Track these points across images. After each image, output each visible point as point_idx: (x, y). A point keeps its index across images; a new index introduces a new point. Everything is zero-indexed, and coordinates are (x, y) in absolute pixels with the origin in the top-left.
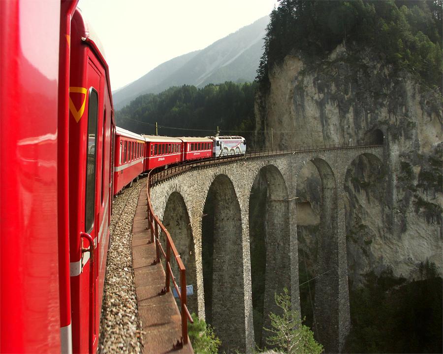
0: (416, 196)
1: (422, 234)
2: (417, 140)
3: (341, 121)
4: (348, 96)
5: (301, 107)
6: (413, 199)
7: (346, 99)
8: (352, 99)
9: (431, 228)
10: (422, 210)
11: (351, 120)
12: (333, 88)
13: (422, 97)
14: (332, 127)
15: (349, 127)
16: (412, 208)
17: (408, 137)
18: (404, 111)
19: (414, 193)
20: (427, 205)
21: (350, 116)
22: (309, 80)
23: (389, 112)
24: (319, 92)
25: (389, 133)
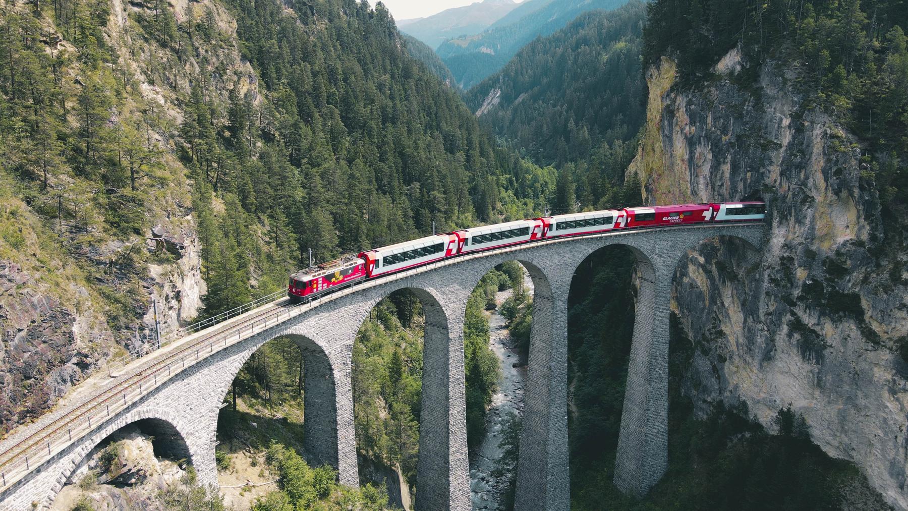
0: (793, 314)
1: (792, 370)
2: (812, 228)
3: (711, 173)
5: (669, 139)
6: (789, 316)
8: (731, 143)
9: (807, 367)
10: (797, 336)
11: (727, 175)
12: (709, 120)
13: (829, 160)
14: (702, 180)
15: (722, 185)
16: (785, 329)
17: (799, 221)
18: (802, 176)
21: (726, 168)
22: (681, 101)
23: (781, 174)
24: (691, 124)
25: (774, 209)
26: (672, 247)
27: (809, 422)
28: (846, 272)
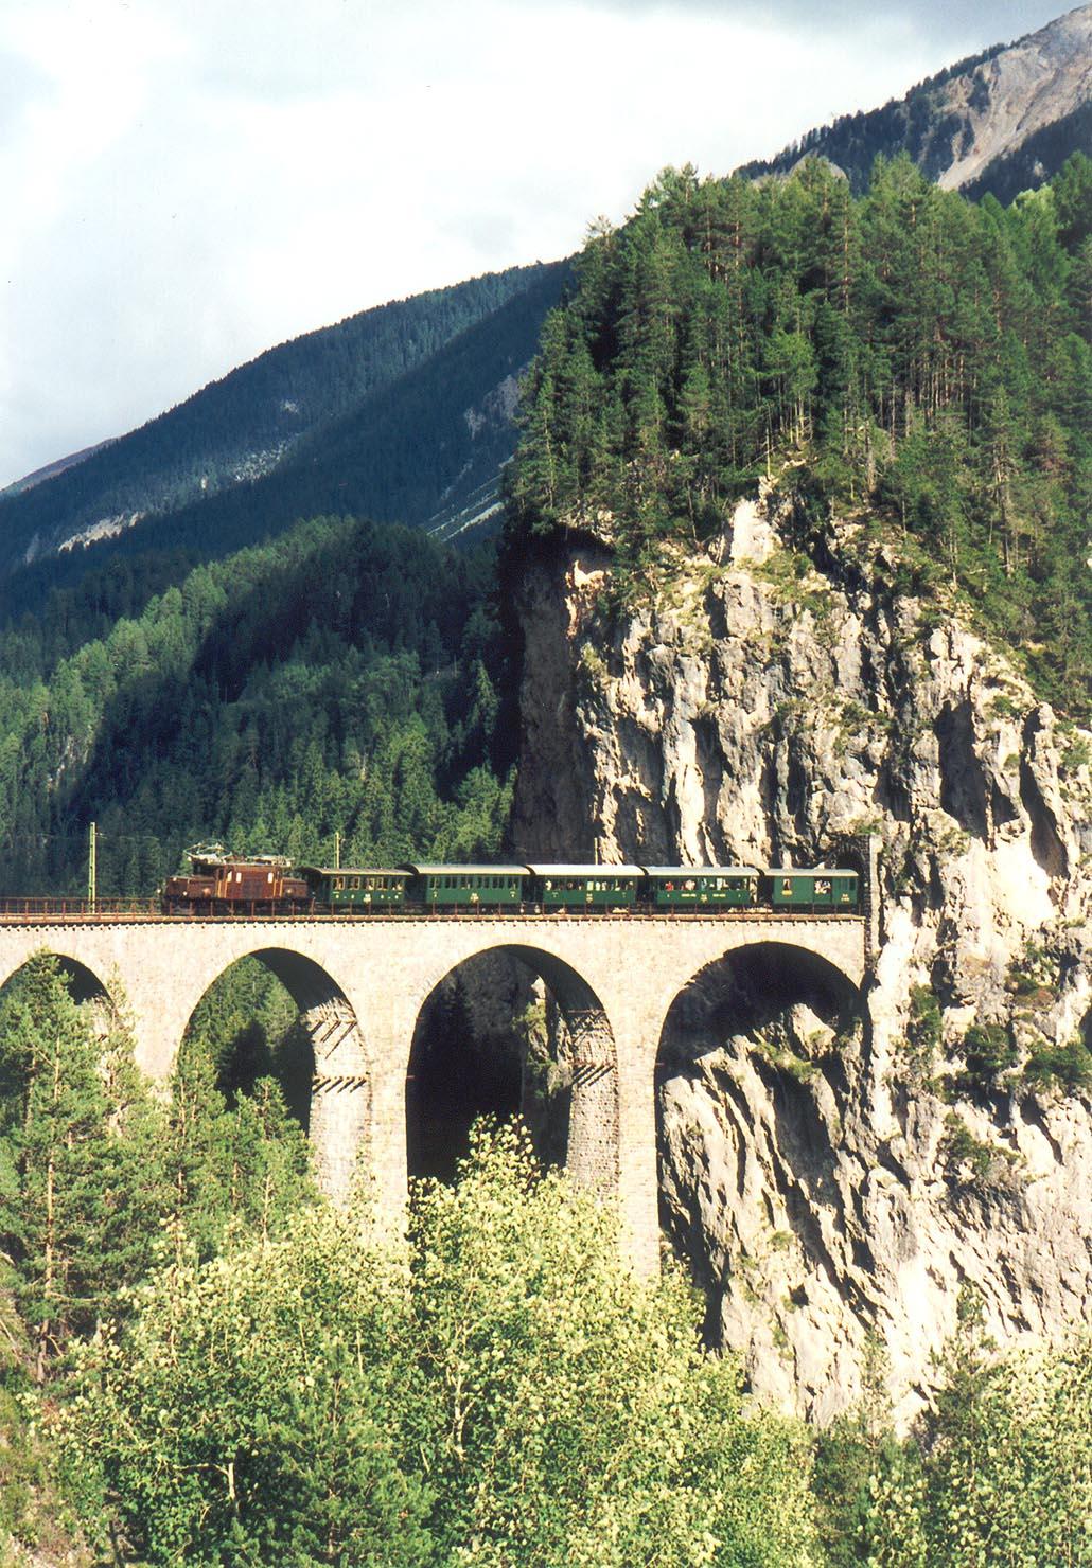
4: (753, 716)
7: (748, 728)
9: (995, 1242)
19: (948, 1109)
20: (983, 1154)
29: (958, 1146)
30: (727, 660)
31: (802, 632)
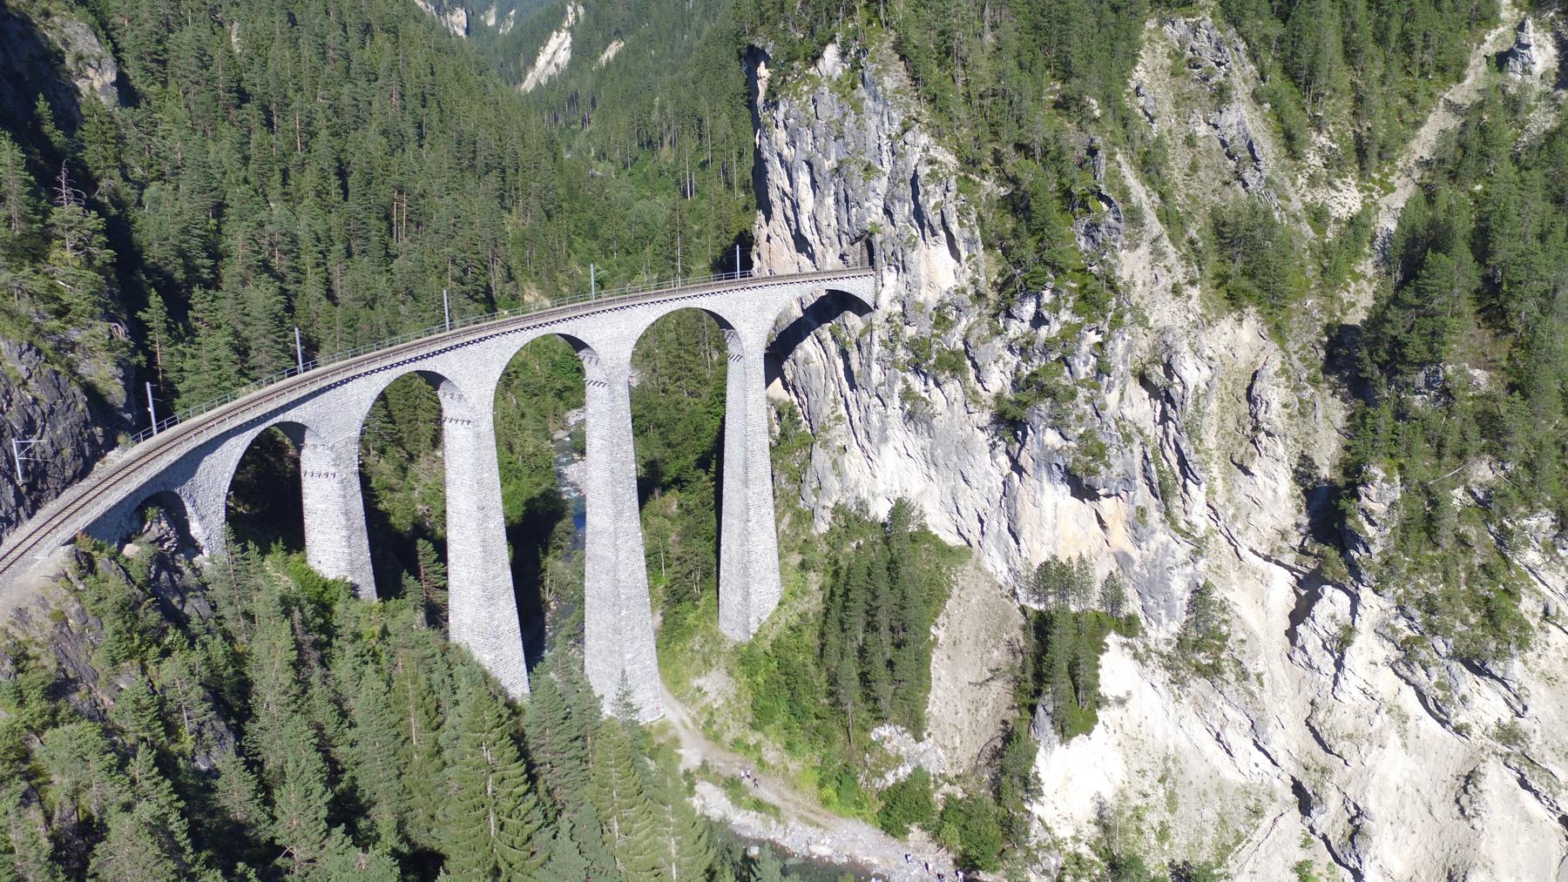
11: (833, 213)
16: (897, 402)
20: (918, 398)
21: (830, 201)
26: (760, 309)
27: (927, 508)
28: (952, 325)
29: (907, 394)
30: (818, 132)
31: (849, 123)
